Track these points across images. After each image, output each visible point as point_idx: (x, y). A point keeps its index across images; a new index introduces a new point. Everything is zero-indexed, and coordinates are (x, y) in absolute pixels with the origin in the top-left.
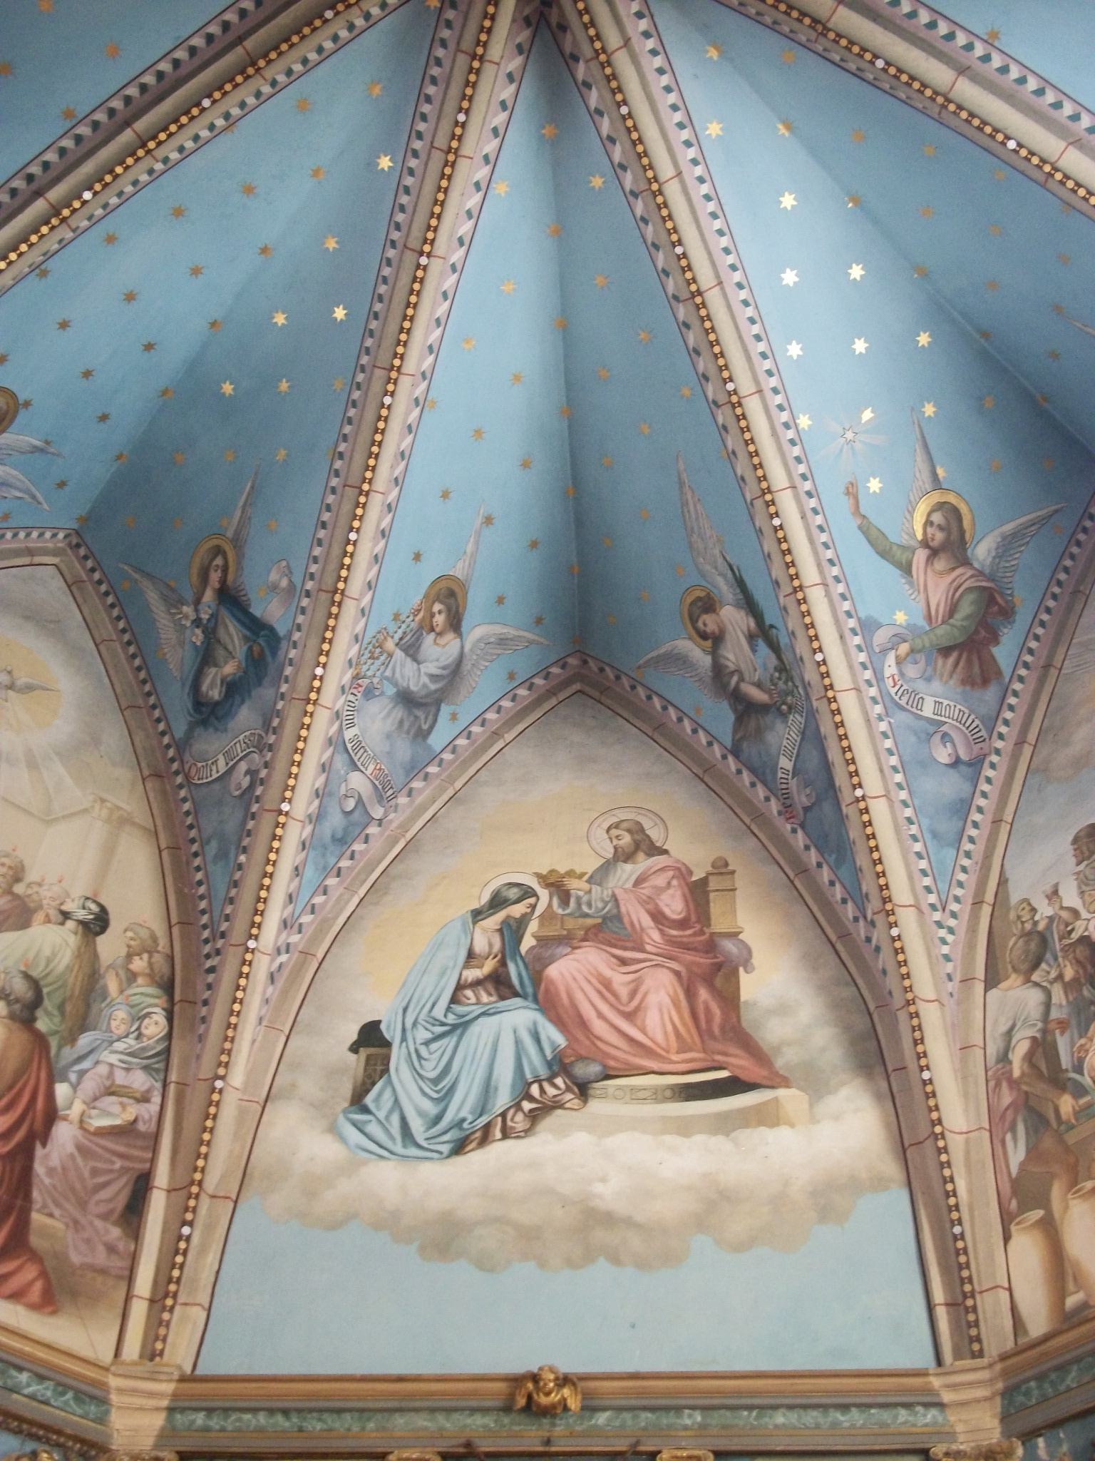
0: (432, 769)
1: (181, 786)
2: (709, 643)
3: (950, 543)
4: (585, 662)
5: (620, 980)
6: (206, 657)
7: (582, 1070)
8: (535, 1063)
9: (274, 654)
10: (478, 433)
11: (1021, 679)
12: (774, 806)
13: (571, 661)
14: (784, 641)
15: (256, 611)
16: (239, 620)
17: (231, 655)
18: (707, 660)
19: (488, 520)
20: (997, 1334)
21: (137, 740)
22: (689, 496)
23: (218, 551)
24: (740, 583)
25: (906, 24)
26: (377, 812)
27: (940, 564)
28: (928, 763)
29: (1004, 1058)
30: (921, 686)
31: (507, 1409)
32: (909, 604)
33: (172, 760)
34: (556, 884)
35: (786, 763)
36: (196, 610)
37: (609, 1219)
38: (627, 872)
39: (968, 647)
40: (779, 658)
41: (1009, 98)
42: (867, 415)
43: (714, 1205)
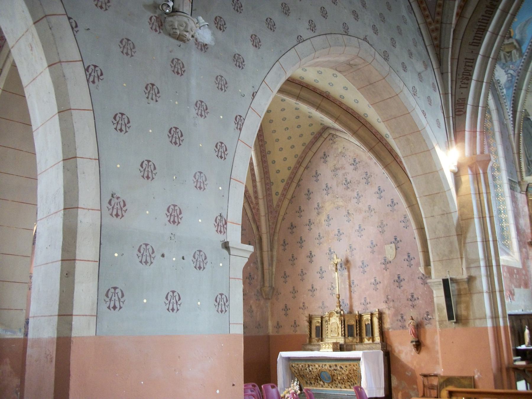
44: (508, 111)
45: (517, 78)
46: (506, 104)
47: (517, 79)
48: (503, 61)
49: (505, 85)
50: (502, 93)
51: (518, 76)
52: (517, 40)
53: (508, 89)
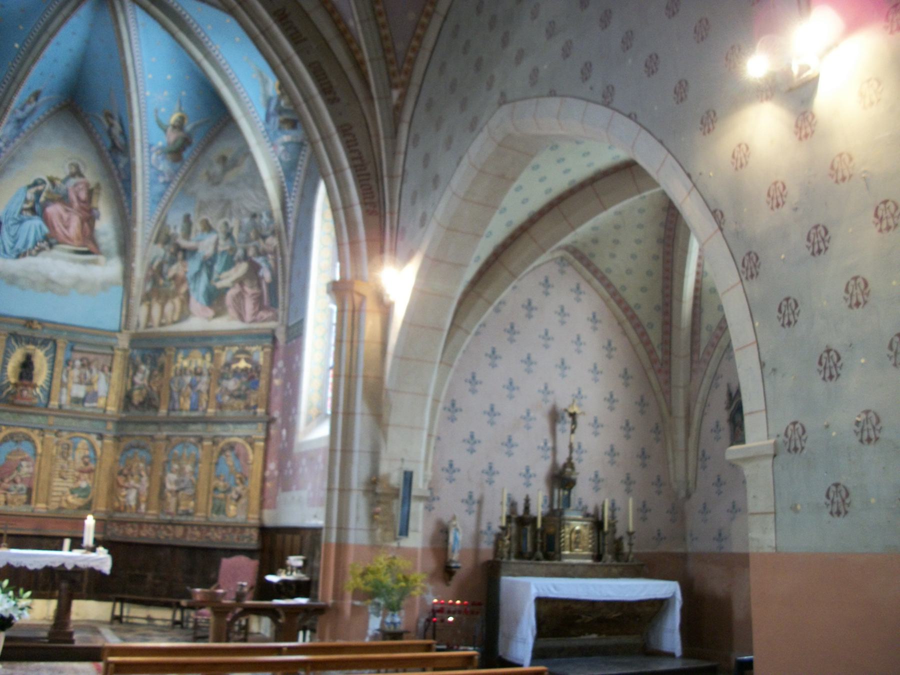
3: (179, 126)
5: (65, 216)
7: (53, 241)
8: (40, 236)
12: (116, 173)
20: (133, 331)
29: (152, 263)
31: (25, 326)
32: (163, 140)
34: (52, 181)
35: (121, 165)
37: (53, 282)
38: (73, 181)
39: (176, 153)
43: (78, 282)
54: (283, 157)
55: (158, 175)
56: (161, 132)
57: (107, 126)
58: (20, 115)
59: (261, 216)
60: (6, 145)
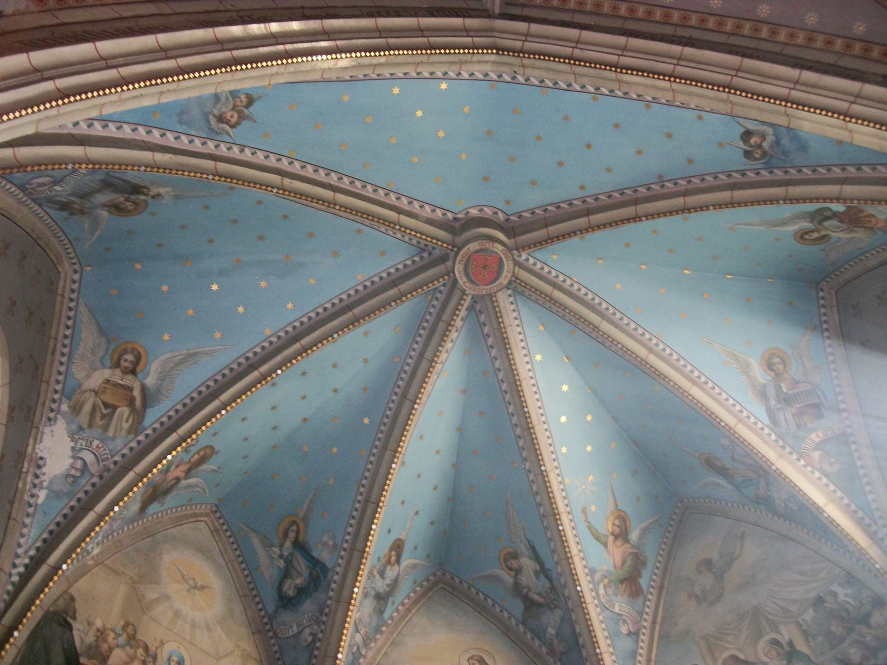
0: (384, 629)
1: (271, 638)
2: (513, 573)
3: (622, 535)
4: (444, 574)
6: (286, 574)
9: (325, 577)
10: (419, 476)
11: (651, 594)
12: (544, 650)
13: (438, 573)
14: (554, 576)
15: (315, 554)
16: (304, 557)
17: (300, 574)
18: (510, 580)
19: (417, 513)
21: (249, 614)
22: (510, 508)
23: (294, 523)
24: (533, 548)
25: (625, 327)
26: (363, 652)
27: (619, 542)
28: (618, 634)
30: (613, 597)
33: (266, 624)
35: (551, 631)
36: (281, 551)
40: (552, 584)
41: (667, 362)
42: (591, 478)
44: (20, 551)
45: (95, 480)
46: (25, 531)
47: (93, 485)
48: (84, 418)
49: (51, 482)
50: (33, 496)
51: (101, 477)
52: (143, 388)
53: (55, 494)
54: (827, 468)
55: (617, 622)
56: (600, 547)
57: (509, 579)
58: (381, 585)
59: (835, 595)
60: (366, 643)
